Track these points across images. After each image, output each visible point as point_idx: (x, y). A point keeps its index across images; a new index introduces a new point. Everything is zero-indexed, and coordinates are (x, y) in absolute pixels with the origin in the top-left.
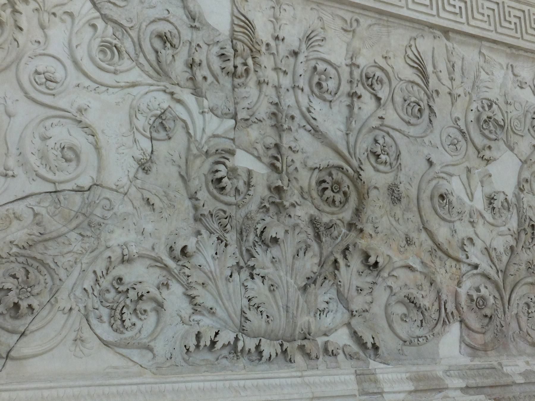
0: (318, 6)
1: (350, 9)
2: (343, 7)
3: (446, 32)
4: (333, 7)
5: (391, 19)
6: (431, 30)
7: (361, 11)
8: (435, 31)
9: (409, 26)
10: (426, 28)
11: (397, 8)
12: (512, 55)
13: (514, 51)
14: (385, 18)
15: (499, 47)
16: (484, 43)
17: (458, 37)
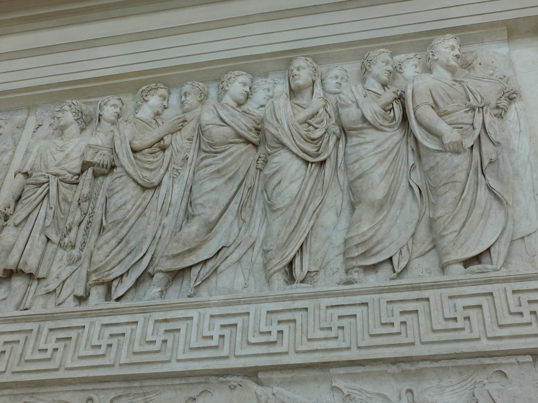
0: (32, 397)
1: (78, 388)
2: (68, 388)
3: (252, 373)
4: (53, 392)
5: (146, 383)
6: (221, 379)
7: (98, 386)
8: (228, 379)
9: (180, 384)
10: (213, 379)
11: (159, 365)
12: (406, 374)
13: (406, 366)
14: (136, 384)
15: (368, 369)
16: (333, 371)
17: (277, 376)
